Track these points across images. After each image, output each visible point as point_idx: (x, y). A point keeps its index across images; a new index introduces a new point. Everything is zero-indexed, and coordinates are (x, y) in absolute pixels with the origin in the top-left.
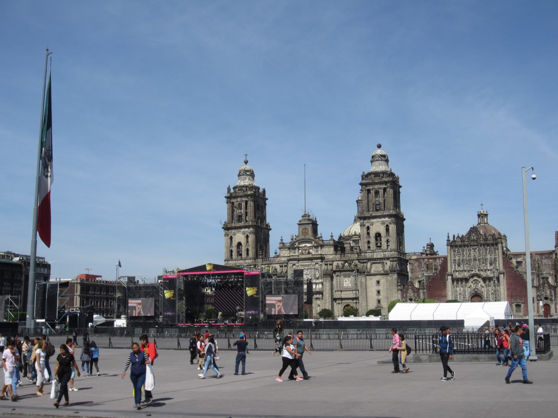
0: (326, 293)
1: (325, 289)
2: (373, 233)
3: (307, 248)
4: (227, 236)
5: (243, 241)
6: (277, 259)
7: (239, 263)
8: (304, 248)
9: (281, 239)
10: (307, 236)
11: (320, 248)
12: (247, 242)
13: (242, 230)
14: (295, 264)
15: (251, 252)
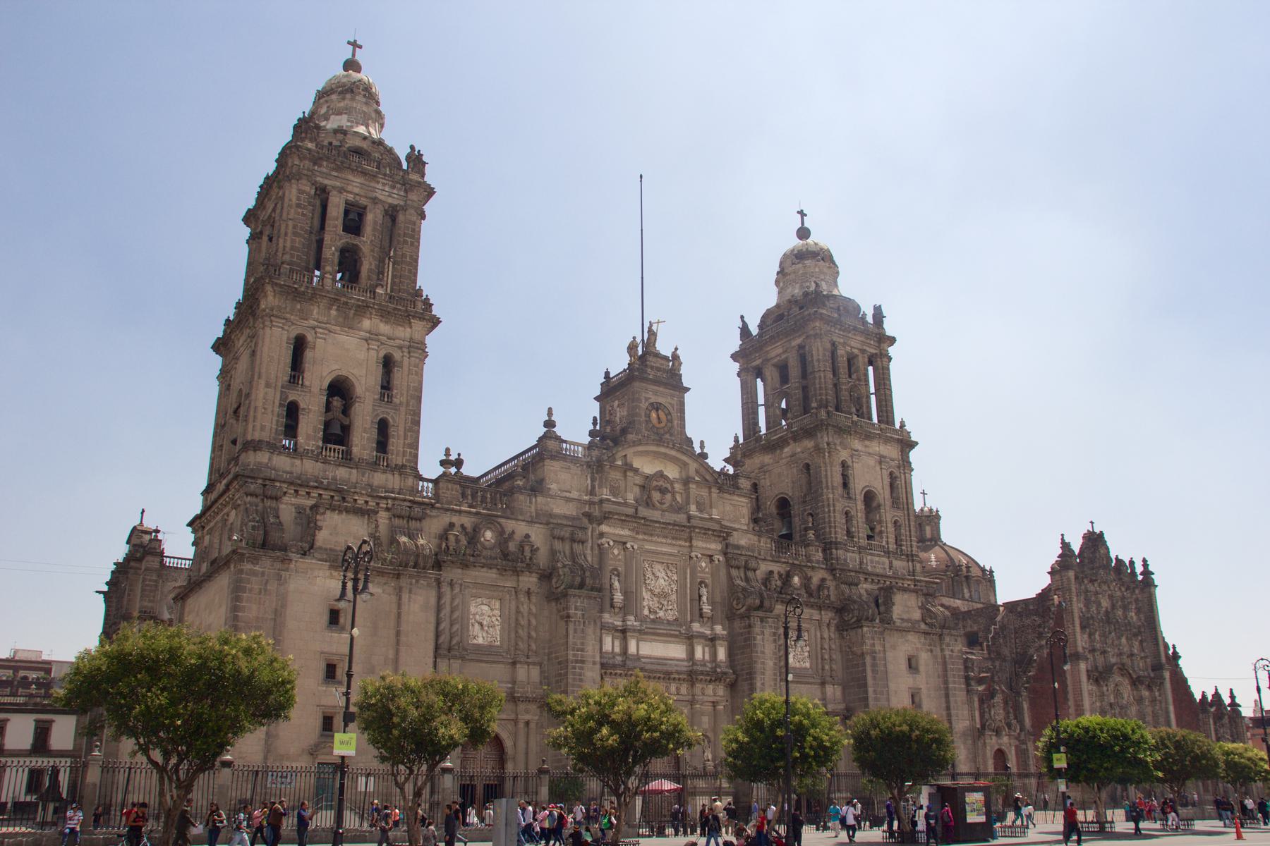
0: (763, 684)
1: (759, 666)
2: (859, 485)
3: (668, 486)
4: (282, 328)
5: (365, 382)
6: (531, 502)
7: (334, 478)
8: (655, 483)
9: (547, 418)
10: (667, 436)
11: (714, 495)
12: (386, 386)
13: (366, 323)
14: (624, 540)
15: (402, 442)
